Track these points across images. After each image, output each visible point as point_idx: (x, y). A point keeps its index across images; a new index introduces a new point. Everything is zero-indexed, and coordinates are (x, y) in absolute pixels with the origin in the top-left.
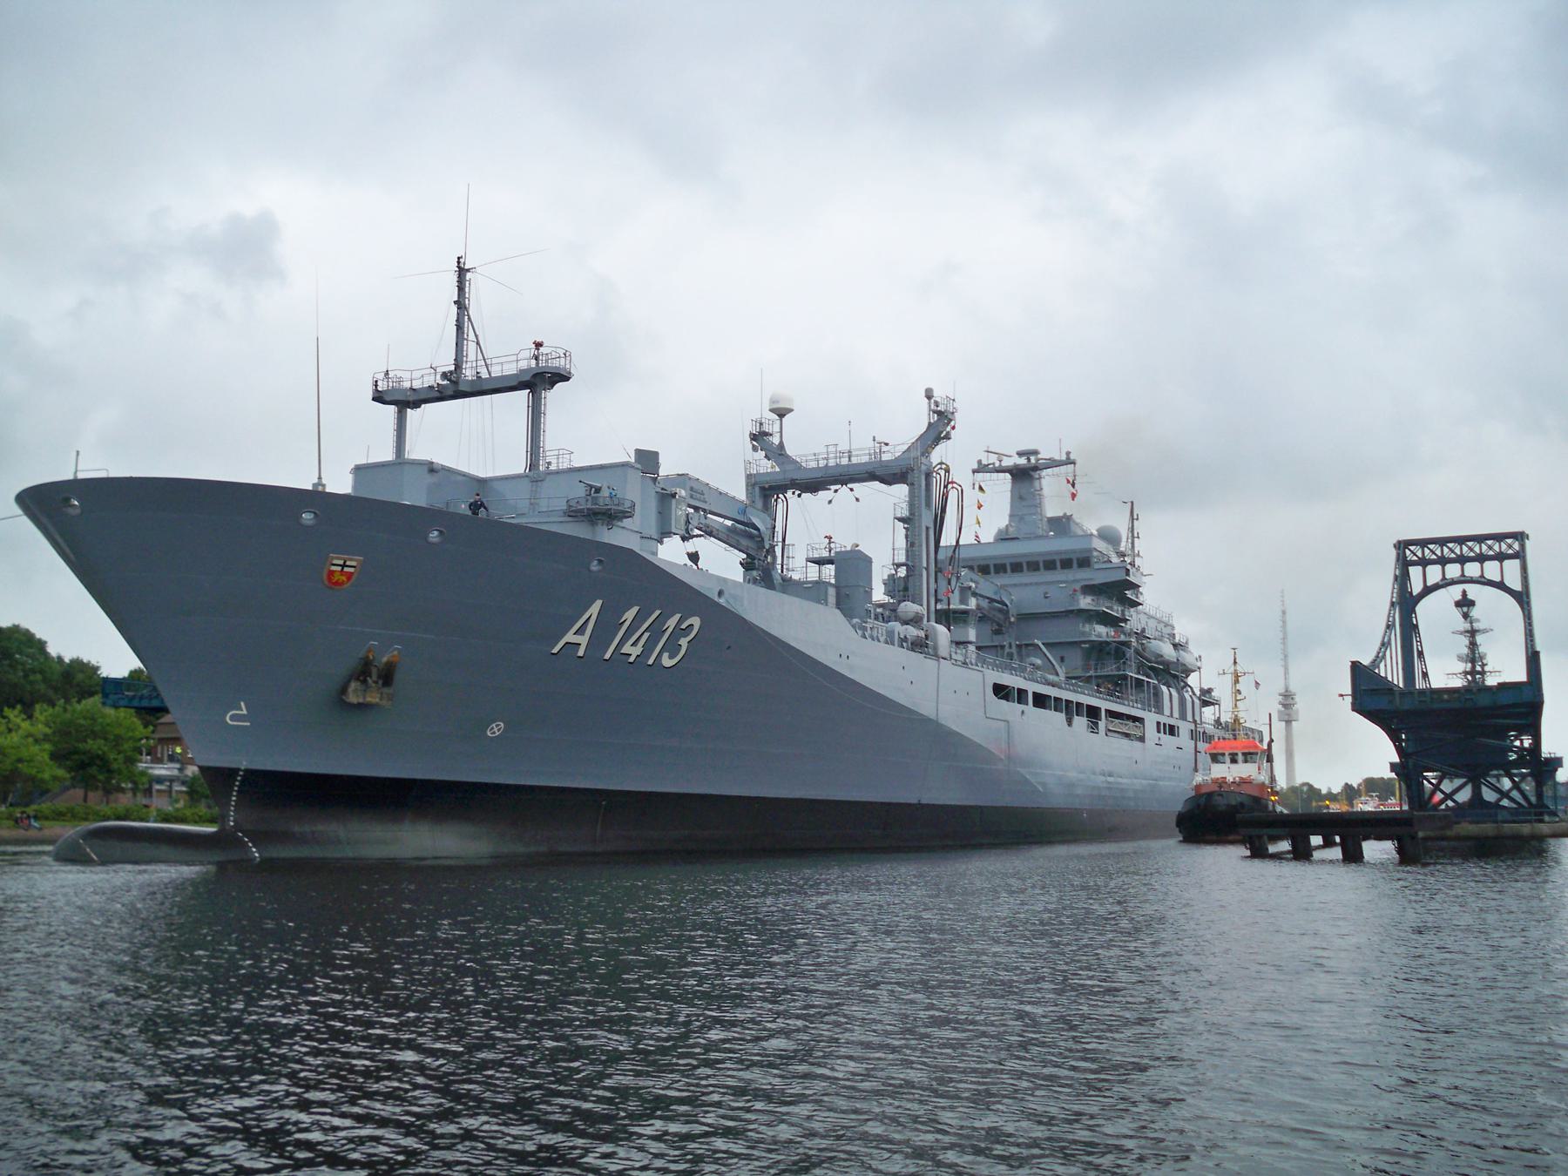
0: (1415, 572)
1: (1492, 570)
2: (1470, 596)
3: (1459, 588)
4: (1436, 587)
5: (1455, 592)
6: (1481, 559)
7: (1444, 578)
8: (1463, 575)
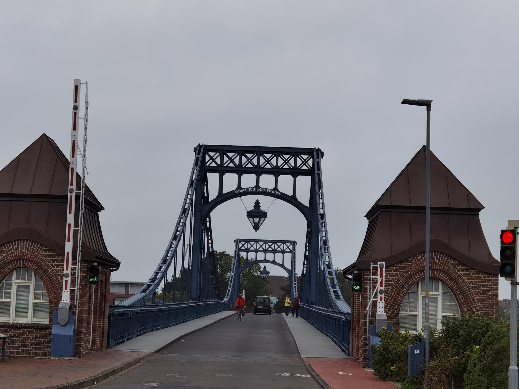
0: (213, 178)
2: (263, 208)
3: (254, 198)
4: (231, 195)
5: (249, 201)
6: (277, 172)
7: (239, 186)
8: (258, 186)
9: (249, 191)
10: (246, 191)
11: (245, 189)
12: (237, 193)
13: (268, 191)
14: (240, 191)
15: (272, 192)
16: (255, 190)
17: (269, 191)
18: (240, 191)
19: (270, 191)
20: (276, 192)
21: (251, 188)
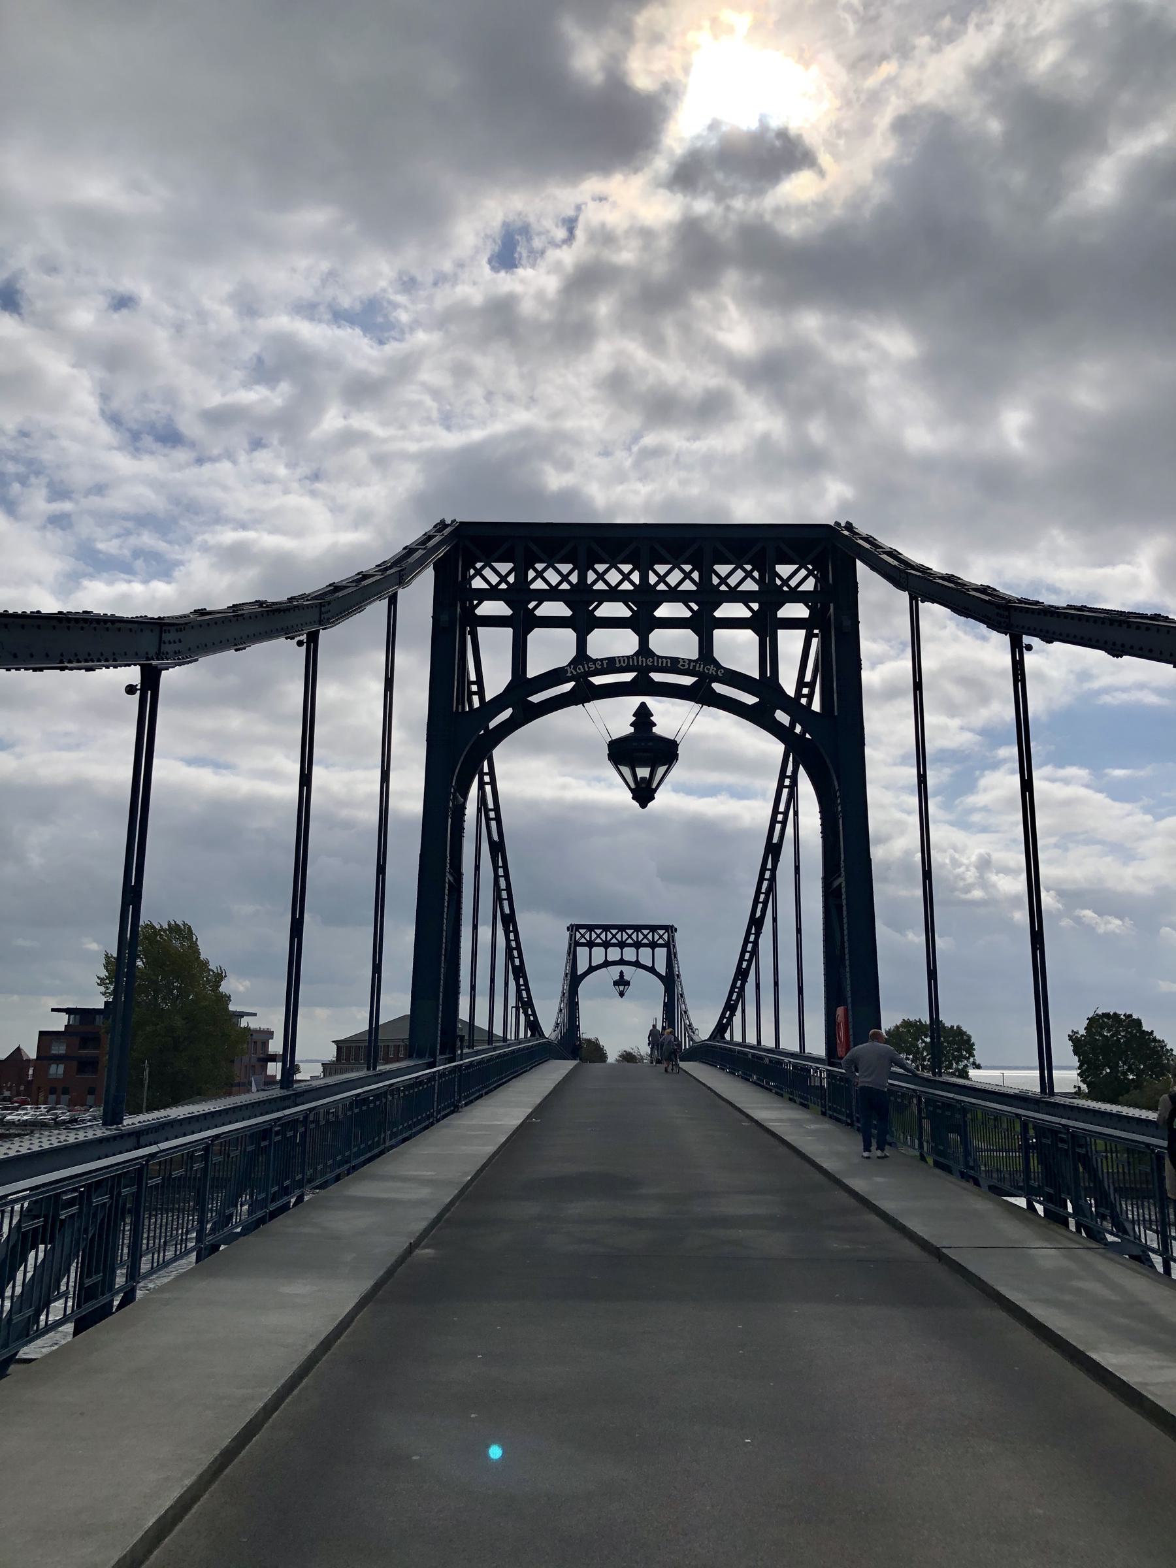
1: (645, 955)
9: (618, 665)
10: (605, 666)
11: (602, 660)
12: (575, 673)
13: (683, 666)
14: (584, 668)
15: (694, 667)
16: (638, 662)
17: (686, 664)
18: (584, 668)
19: (689, 664)
20: (708, 669)
21: (623, 657)
